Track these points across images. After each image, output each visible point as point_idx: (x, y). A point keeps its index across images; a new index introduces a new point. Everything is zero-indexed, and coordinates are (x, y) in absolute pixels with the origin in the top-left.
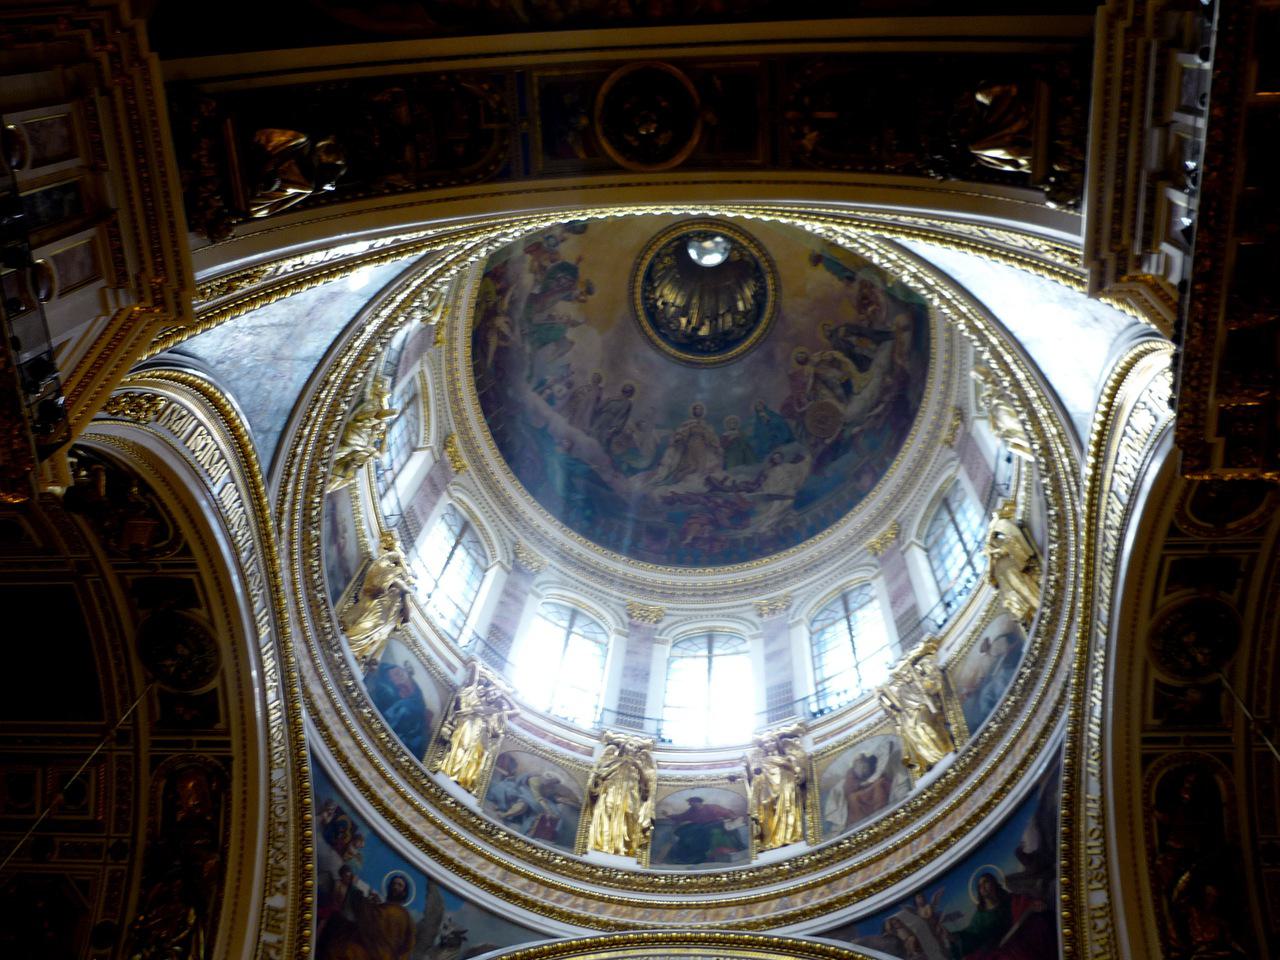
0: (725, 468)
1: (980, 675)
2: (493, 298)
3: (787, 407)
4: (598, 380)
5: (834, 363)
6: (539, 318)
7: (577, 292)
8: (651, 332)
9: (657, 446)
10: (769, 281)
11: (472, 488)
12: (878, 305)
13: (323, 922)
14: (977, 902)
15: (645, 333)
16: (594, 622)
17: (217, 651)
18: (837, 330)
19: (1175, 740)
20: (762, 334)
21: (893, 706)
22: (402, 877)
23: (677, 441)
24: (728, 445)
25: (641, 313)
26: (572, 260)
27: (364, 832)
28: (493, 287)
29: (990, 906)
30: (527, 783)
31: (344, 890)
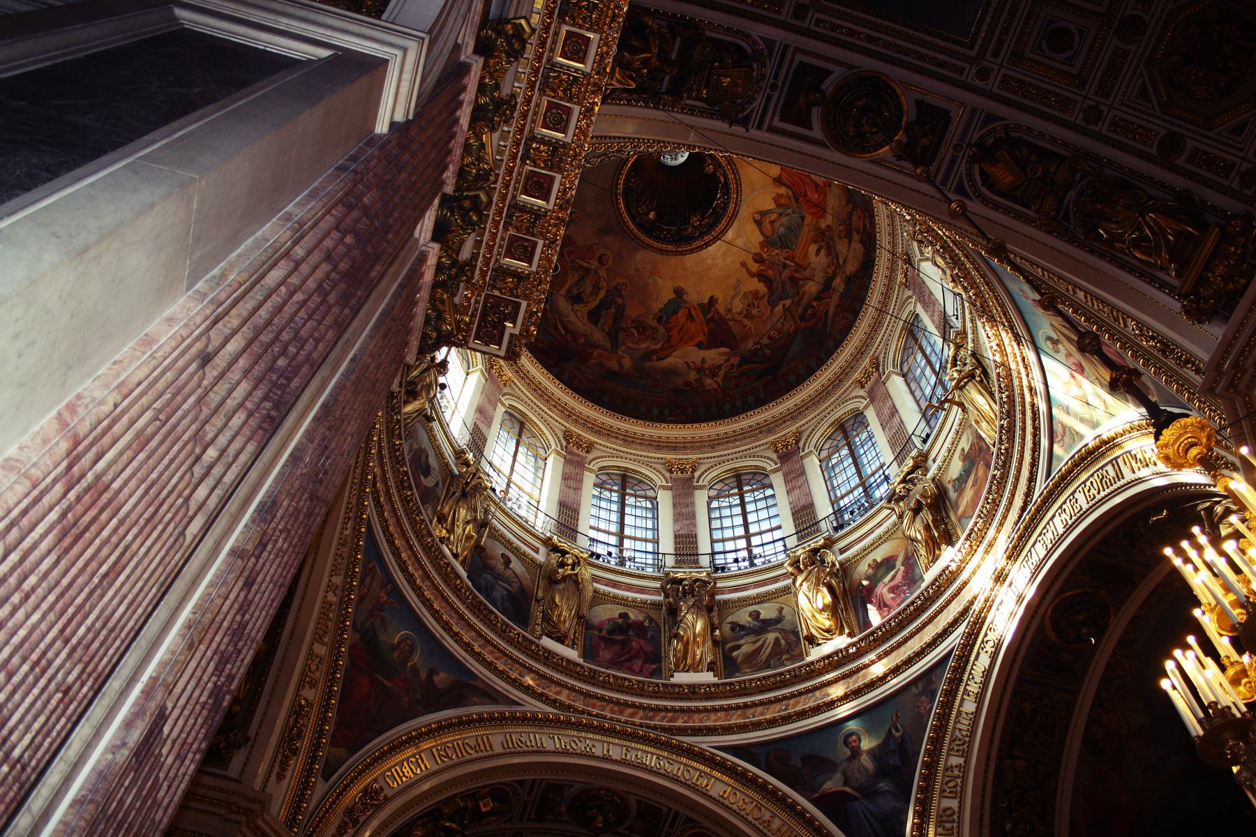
1: (493, 562)
5: (596, 290)
10: (670, 248)
19: (529, 795)
21: (467, 484)
29: (396, 654)
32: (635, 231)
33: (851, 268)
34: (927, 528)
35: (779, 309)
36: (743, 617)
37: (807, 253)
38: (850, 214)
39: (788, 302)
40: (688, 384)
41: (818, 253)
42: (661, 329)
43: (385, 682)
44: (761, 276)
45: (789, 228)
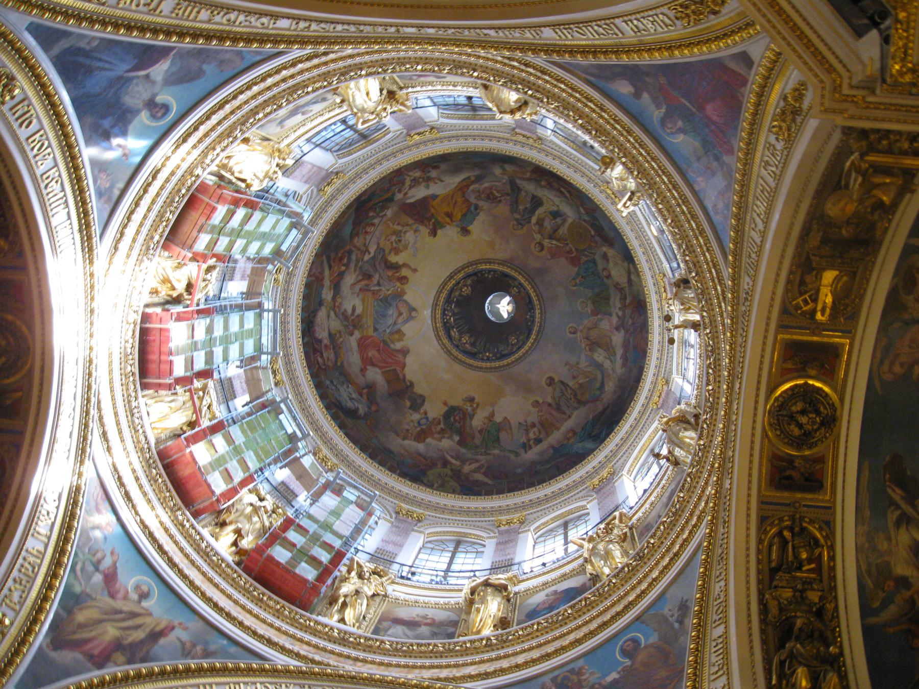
0: (611, 315)
2: (447, 471)
3: (574, 261)
4: (536, 404)
5: (540, 223)
6: (477, 441)
7: (470, 409)
8: (513, 358)
9: (590, 365)
10: (483, 267)
12: (491, 188)
14: (680, 138)
15: (513, 362)
18: (516, 220)
20: (523, 276)
22: (625, 642)
24: (595, 313)
25: (497, 364)
27: (580, 663)
28: (438, 470)
32: (516, 275)
33: (322, 314)
34: (173, 288)
35: (372, 250)
37: (363, 303)
38: (337, 356)
39: (367, 257)
40: (436, 167)
42: (472, 200)
43: (688, 104)
44: (396, 267)
45: (384, 316)
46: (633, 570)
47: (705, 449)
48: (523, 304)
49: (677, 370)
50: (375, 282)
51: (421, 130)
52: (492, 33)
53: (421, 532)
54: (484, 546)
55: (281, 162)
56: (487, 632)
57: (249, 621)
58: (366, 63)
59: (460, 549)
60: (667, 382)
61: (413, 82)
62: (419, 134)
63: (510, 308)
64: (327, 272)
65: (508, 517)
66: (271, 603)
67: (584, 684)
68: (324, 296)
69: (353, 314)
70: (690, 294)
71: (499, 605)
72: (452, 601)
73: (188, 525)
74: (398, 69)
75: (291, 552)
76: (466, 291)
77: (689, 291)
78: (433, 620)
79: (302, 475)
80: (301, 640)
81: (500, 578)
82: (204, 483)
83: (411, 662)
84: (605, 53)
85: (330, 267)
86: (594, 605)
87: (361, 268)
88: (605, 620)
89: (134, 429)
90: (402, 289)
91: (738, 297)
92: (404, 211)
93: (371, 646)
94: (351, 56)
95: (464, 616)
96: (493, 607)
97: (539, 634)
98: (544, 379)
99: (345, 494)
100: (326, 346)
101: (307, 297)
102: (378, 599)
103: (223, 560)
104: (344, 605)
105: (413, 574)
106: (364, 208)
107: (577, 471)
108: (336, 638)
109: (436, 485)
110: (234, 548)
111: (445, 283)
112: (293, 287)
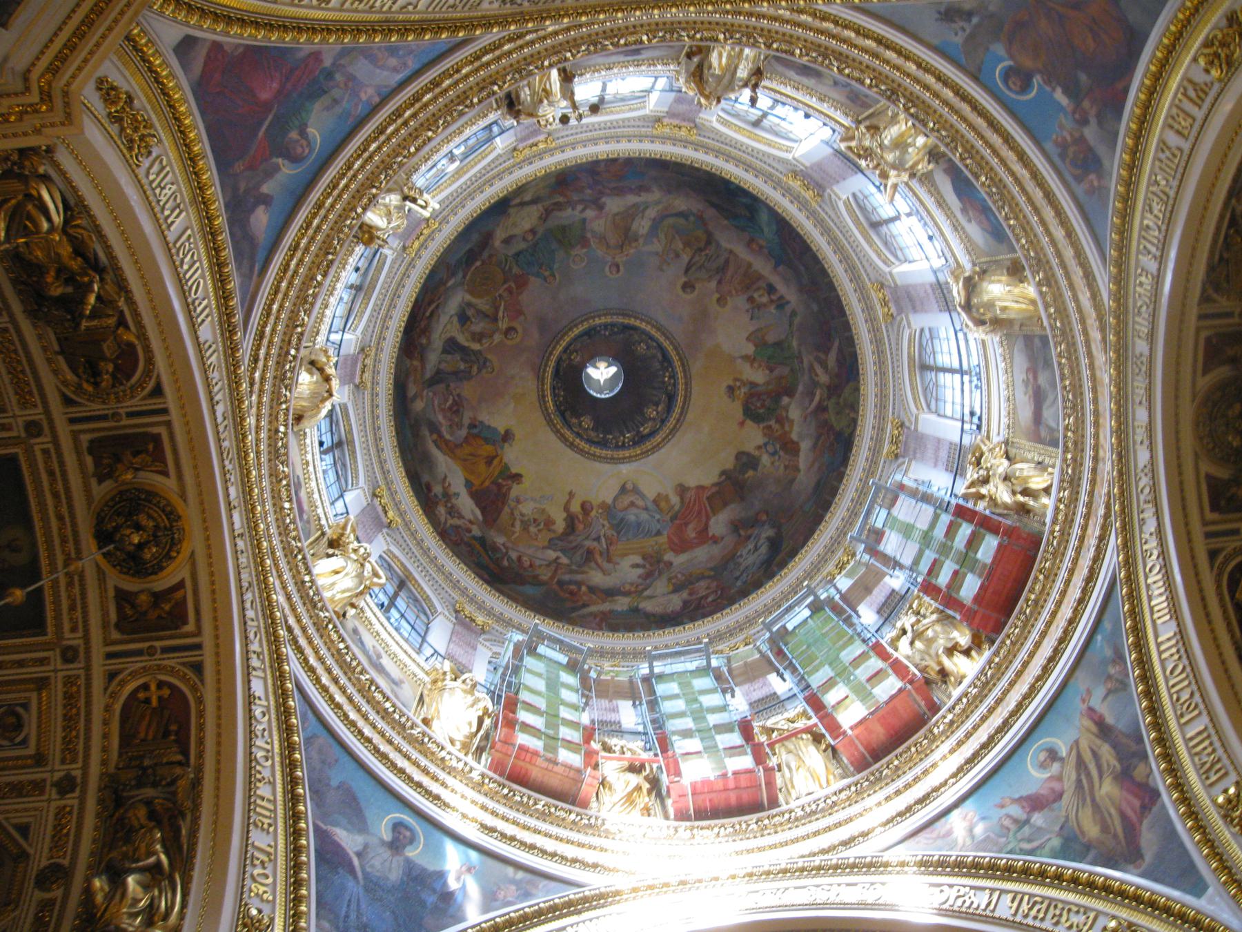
0: (584, 220)
2: (831, 404)
3: (521, 283)
4: (721, 301)
5: (478, 337)
6: (785, 371)
8: (666, 344)
10: (551, 404)
11: (865, 263)
12: (443, 410)
13: (1120, 86)
15: (671, 343)
16: (733, 116)
17: (1197, 424)
18: (479, 370)
19: (130, 415)
20: (554, 348)
23: (636, 240)
24: (584, 242)
25: (677, 364)
26: (749, 422)
27: (1049, 146)
28: (831, 416)
30: (836, 83)
31: (1086, 104)
32: (554, 358)
33: (648, 606)
34: (638, 788)
35: (552, 554)
36: (369, 641)
37: (626, 555)
38: (702, 577)
39: (564, 560)
40: (429, 488)
41: (637, 566)
42: (463, 433)
44: (571, 520)
45: (639, 524)
46: (912, 100)
47: (730, 30)
48: (595, 344)
49: (639, 109)
50: (595, 544)
51: (380, 509)
52: (220, 409)
53: (917, 419)
54: (922, 330)
55: (448, 677)
56: (1031, 291)
57: (1066, 612)
58: (294, 577)
59: (932, 363)
60: (658, 120)
61: (312, 519)
62: (386, 513)
63: (602, 365)
64: (593, 609)
65: (878, 307)
66: (1038, 587)
67: (1077, 135)
68: (625, 608)
69: (644, 566)
70: (526, 94)
71: (993, 282)
72: (999, 351)
73: (950, 717)
74: (294, 534)
75: (965, 576)
76: (587, 422)
77: (522, 95)
78: (1028, 370)
79: (864, 588)
80: (1082, 539)
81: (957, 292)
82: (891, 705)
83: (1087, 384)
84: (217, 250)
85: (584, 606)
86: (968, 147)
87: (580, 566)
88: (985, 125)
89: (831, 807)
90: (600, 506)
91: (513, 15)
92: (495, 521)
93: (1075, 443)
94: (289, 598)
95: (1017, 328)
96: (997, 290)
97: (1021, 216)
98: (684, 296)
99: (879, 525)
100: (690, 594)
101: (630, 628)
102: (1012, 452)
103: (990, 662)
104: (1026, 492)
105: (972, 414)
106: (500, 573)
107: (800, 225)
108: (1071, 493)
109: (852, 415)
110: (973, 653)
111: (581, 452)
112: (618, 648)
